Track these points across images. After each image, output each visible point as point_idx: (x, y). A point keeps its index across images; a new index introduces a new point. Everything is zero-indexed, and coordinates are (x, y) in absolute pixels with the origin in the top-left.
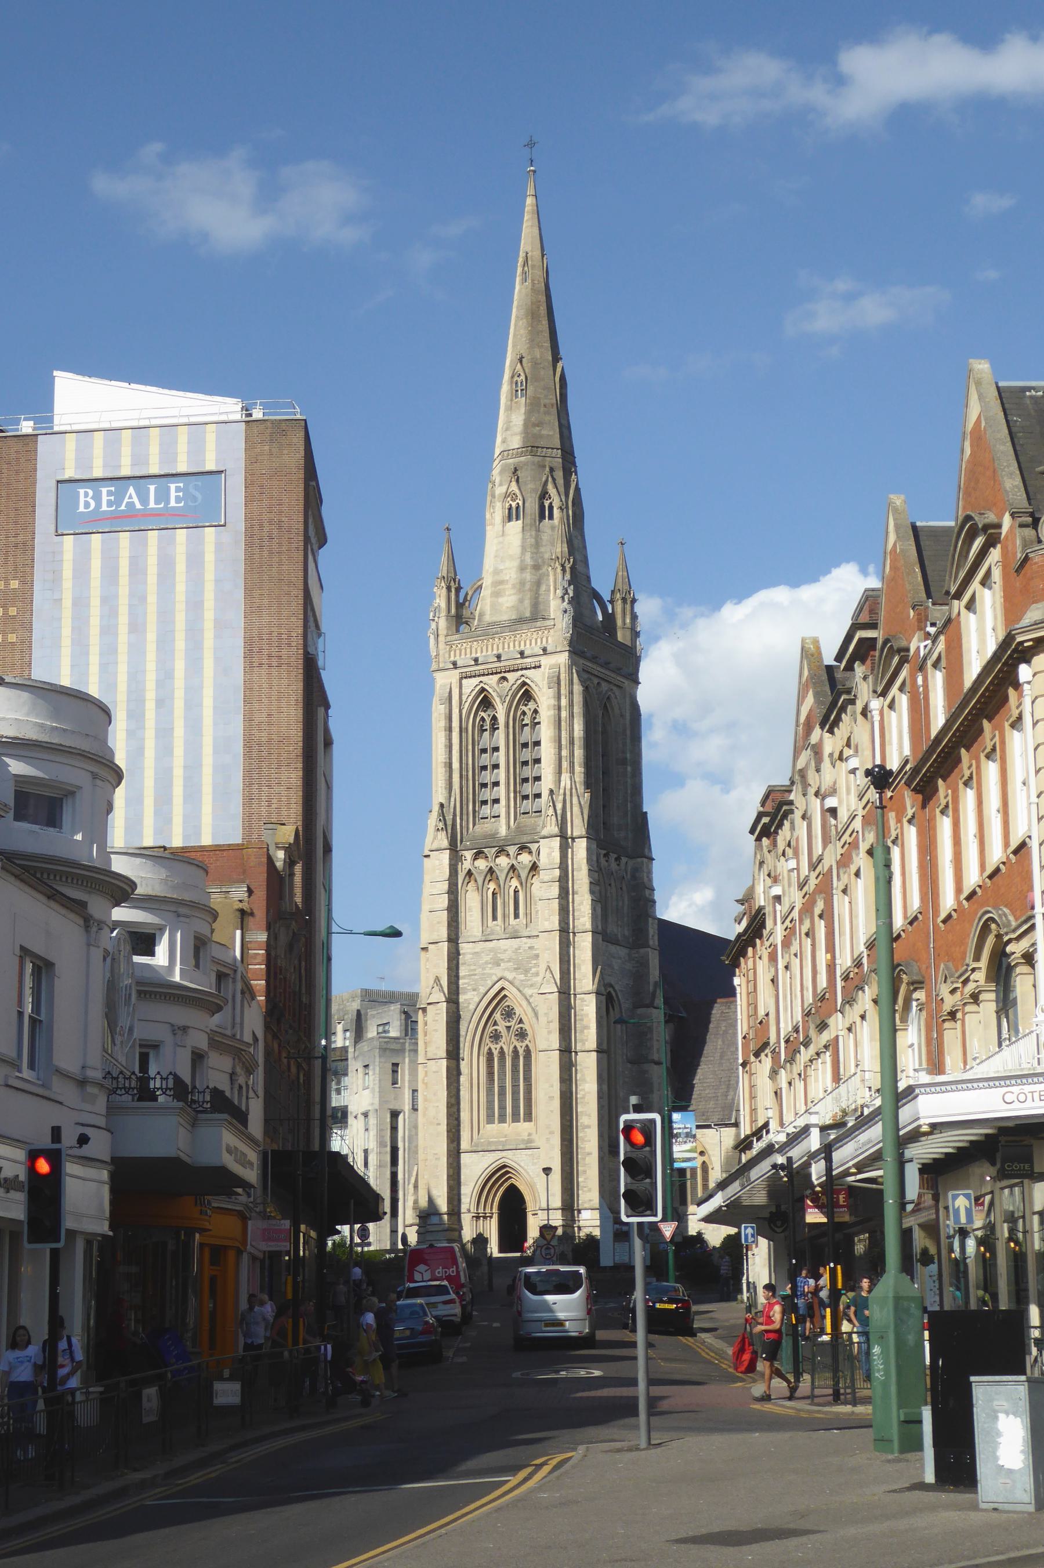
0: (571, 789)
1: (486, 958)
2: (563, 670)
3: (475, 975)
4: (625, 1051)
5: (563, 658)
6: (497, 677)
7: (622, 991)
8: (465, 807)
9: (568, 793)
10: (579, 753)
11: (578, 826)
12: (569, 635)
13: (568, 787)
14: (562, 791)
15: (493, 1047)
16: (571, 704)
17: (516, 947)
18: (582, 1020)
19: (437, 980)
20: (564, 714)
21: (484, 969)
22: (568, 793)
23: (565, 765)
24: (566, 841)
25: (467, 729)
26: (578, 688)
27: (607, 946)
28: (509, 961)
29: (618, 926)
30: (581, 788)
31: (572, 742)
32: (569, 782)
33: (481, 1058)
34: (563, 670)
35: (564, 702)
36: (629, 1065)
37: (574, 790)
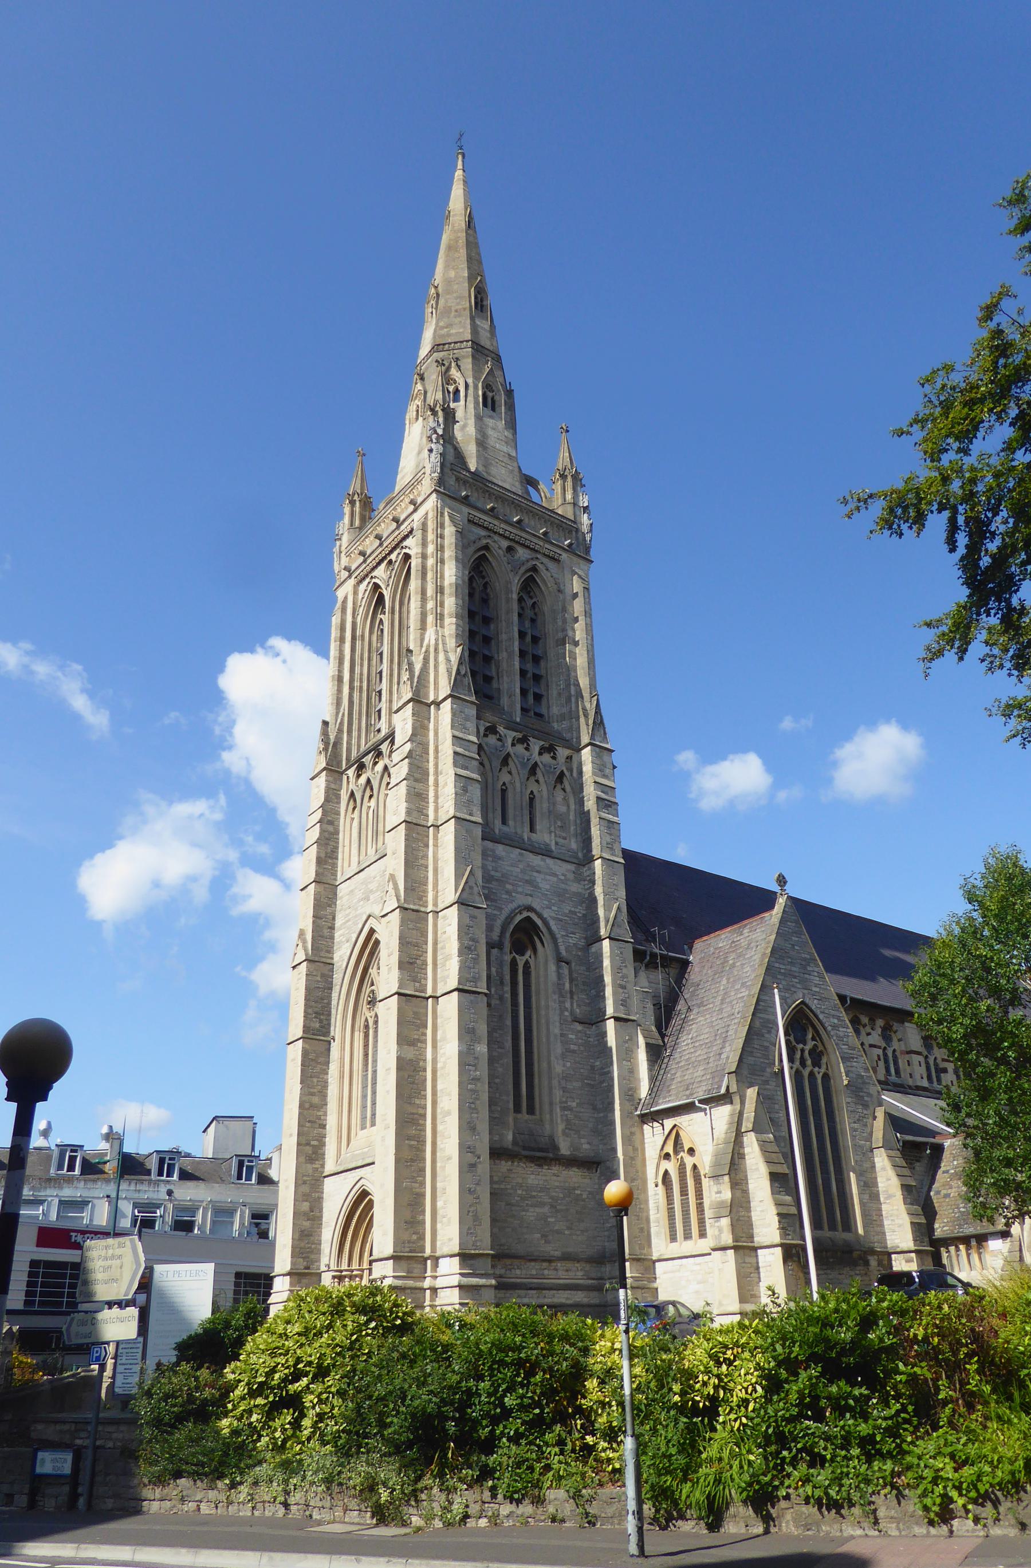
0: (437, 645)
1: (359, 894)
2: (430, 515)
3: (349, 921)
4: (568, 1005)
5: (431, 503)
6: (383, 565)
7: (554, 919)
8: (355, 722)
9: (432, 650)
10: (450, 603)
11: (441, 686)
12: (436, 474)
13: (433, 642)
14: (424, 649)
15: (368, 1015)
16: (440, 548)
17: (383, 868)
18: (443, 948)
19: (302, 934)
20: (431, 562)
21: (356, 909)
22: (432, 650)
23: (430, 619)
24: (420, 703)
25: (363, 636)
26: (449, 531)
27: (521, 854)
28: (377, 891)
29: (551, 832)
30: (451, 643)
31: (440, 590)
32: (433, 638)
33: (356, 1034)
34: (430, 515)
35: (431, 549)
36: (579, 1027)
37: (440, 646)
